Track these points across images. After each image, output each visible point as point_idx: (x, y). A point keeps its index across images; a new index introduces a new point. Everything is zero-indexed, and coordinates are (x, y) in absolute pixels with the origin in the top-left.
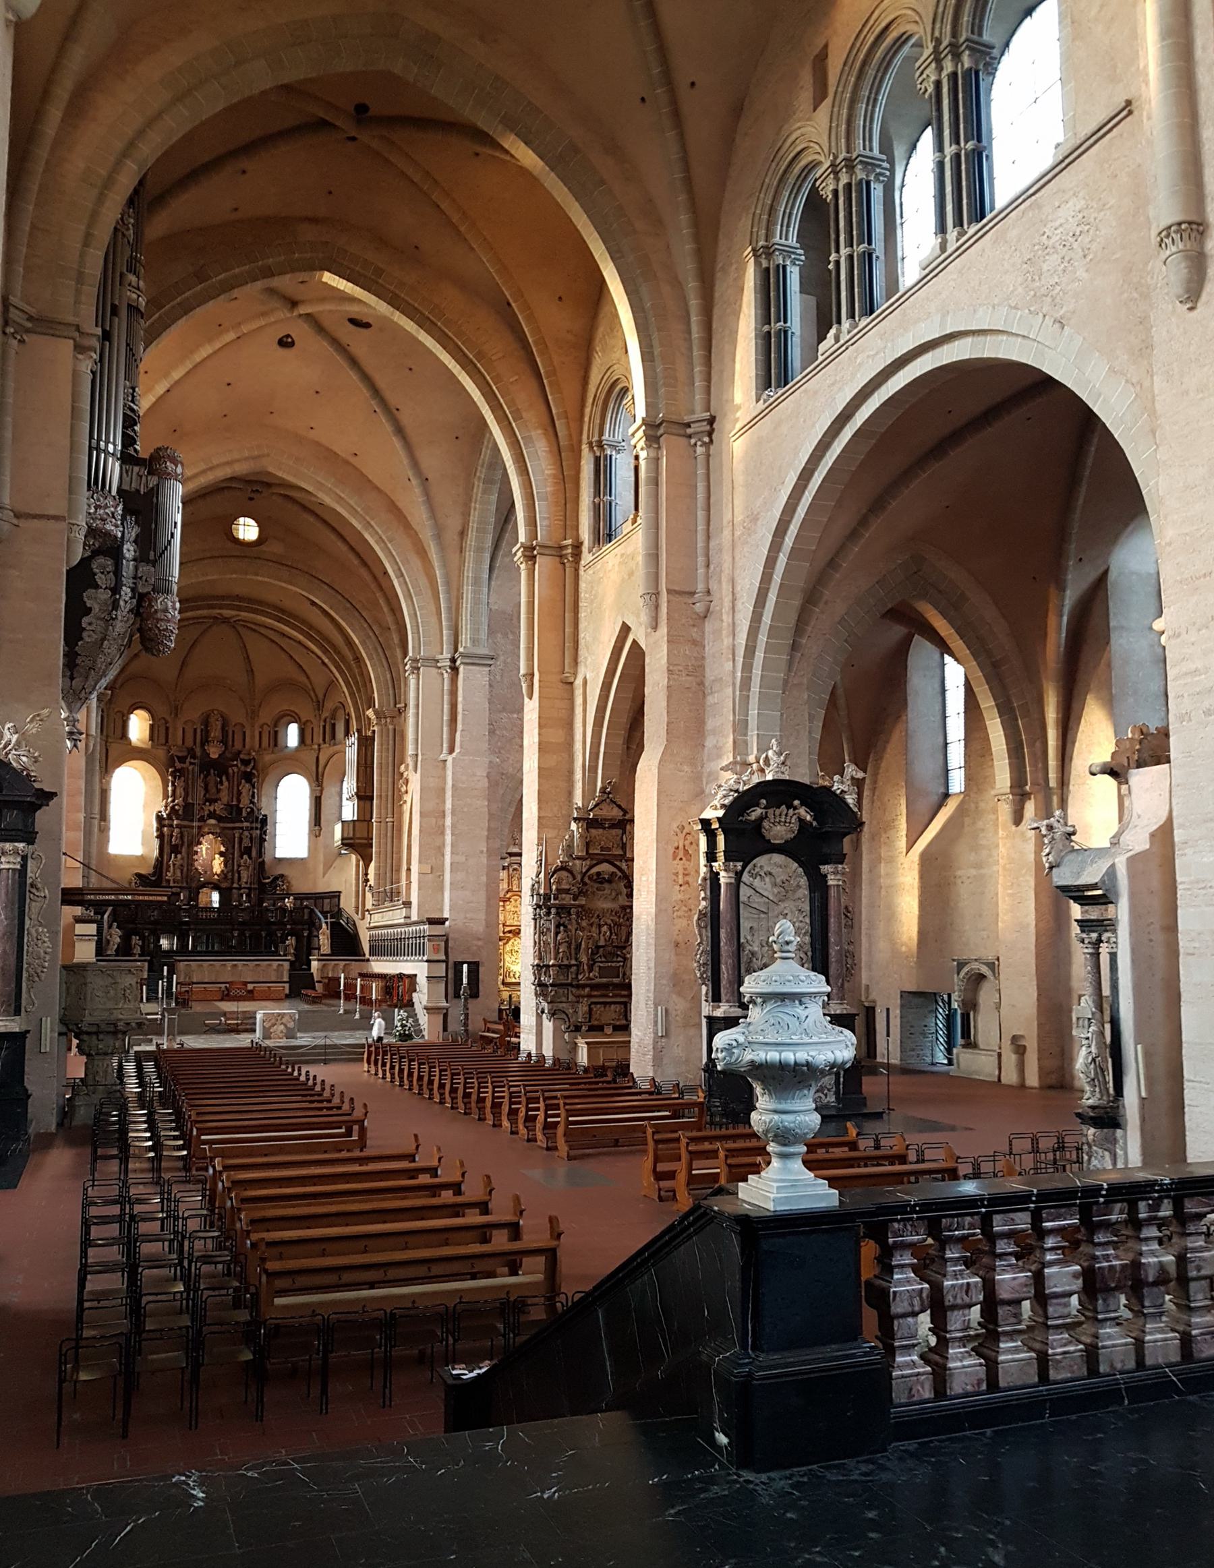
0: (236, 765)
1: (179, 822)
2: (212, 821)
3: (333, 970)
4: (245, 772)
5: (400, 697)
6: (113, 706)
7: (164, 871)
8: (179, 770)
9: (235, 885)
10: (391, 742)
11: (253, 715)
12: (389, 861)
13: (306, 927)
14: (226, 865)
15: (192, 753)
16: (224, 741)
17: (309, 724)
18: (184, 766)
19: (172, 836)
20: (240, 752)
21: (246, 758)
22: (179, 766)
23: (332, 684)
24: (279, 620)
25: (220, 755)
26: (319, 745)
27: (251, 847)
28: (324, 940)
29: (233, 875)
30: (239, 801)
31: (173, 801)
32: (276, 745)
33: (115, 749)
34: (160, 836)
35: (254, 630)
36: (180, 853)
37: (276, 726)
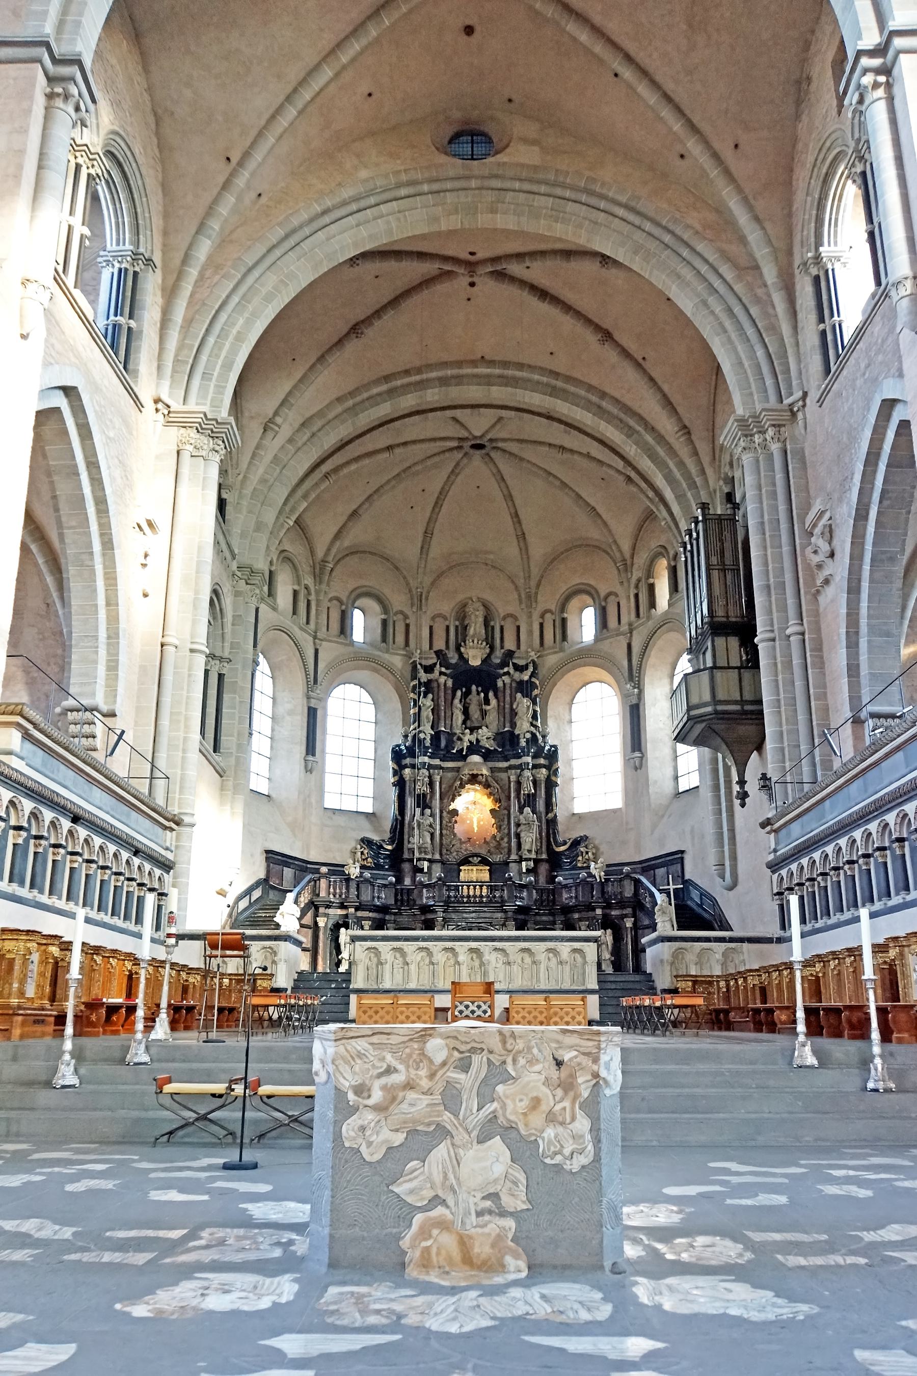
0: (508, 673)
1: (426, 759)
2: (476, 758)
4: (521, 683)
5: (790, 386)
7: (406, 837)
10: (779, 476)
11: (530, 599)
12: (802, 717)
13: (629, 911)
14: (499, 828)
15: (445, 662)
16: (489, 641)
17: (612, 598)
18: (430, 676)
20: (510, 654)
21: (522, 662)
22: (423, 676)
25: (484, 661)
26: (630, 624)
27: (534, 795)
29: (509, 842)
30: (513, 725)
32: (564, 637)
34: (400, 784)
35: (522, 459)
37: (563, 608)
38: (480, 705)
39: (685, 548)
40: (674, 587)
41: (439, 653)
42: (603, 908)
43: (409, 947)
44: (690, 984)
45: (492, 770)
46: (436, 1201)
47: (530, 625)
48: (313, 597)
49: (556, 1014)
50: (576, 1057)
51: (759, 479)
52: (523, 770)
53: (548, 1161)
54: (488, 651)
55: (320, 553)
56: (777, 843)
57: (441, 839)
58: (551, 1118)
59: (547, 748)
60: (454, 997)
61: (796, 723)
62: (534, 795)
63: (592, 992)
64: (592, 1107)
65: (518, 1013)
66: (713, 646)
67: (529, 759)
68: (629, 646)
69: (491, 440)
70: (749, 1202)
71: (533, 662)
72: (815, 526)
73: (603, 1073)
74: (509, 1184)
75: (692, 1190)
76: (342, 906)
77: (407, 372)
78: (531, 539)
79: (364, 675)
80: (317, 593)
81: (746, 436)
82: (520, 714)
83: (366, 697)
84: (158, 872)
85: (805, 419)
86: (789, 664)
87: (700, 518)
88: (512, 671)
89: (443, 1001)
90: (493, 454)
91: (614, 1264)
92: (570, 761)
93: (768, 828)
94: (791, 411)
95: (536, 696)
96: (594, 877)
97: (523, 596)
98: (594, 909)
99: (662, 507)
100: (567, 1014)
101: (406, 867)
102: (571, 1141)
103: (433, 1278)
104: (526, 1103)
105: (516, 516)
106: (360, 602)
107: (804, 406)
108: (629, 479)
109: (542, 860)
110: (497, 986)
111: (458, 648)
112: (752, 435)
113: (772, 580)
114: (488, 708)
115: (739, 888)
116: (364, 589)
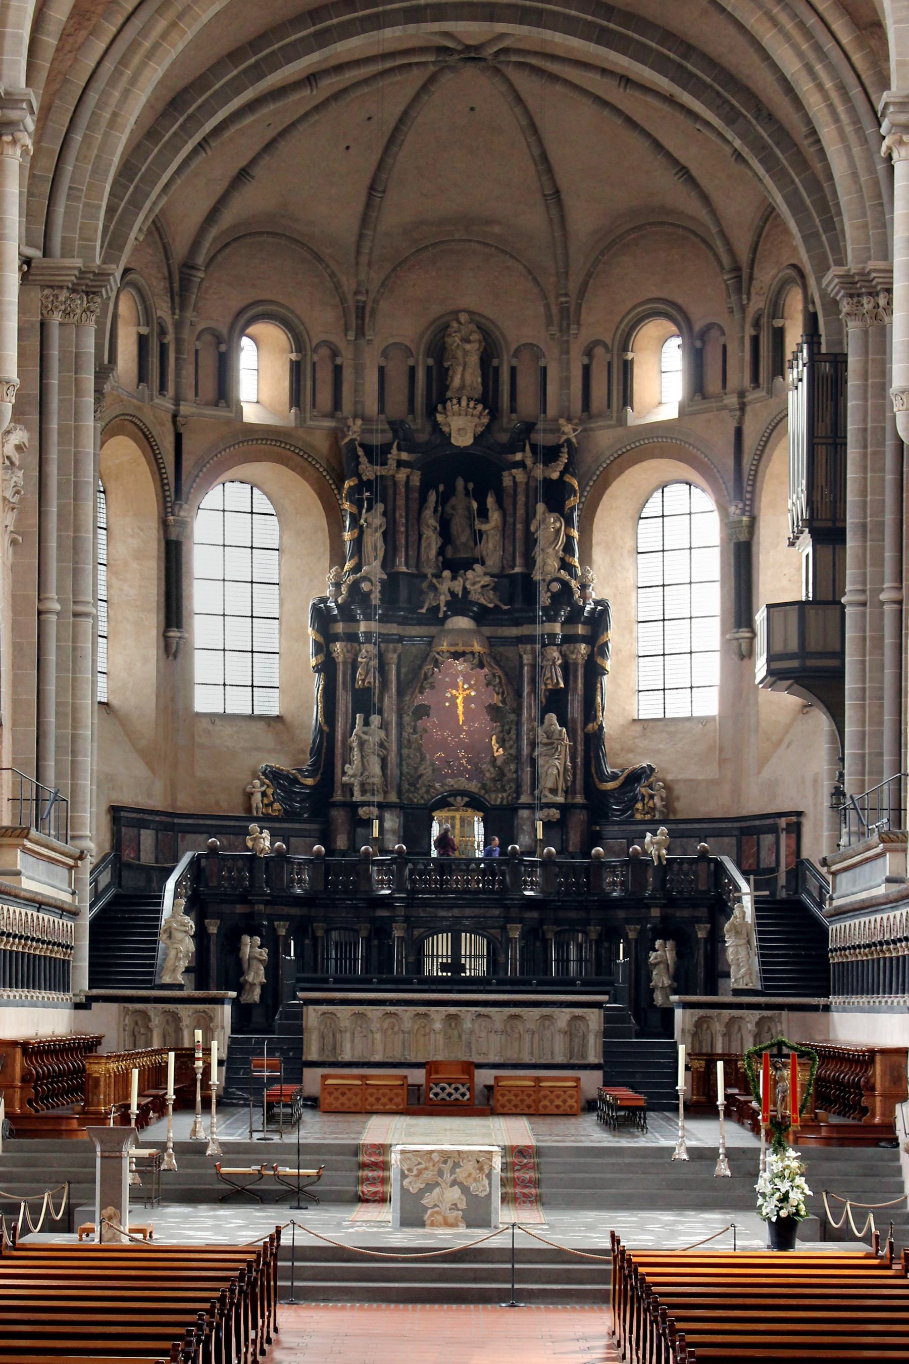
0: (521, 464)
1: (374, 626)
2: (462, 622)
3: (727, 1035)
4: (547, 482)
6: (189, 314)
8: (367, 485)
9: (524, 799)
13: (703, 912)
17: (714, 333)
18: (379, 470)
19: (355, 666)
22: (368, 471)
23: (769, 213)
24: (603, 37)
25: (477, 438)
26: (742, 394)
27: (566, 690)
30: (530, 562)
31: (357, 569)
32: (627, 399)
34: (327, 668)
35: (554, 78)
36: (380, 712)
37: (625, 348)
38: (470, 518)
42: (663, 907)
43: (374, 1012)
44: (703, 1063)
45: (491, 642)
46: (436, 1206)
47: (566, 366)
48: (170, 338)
49: (545, 1097)
51: (866, 362)
54: (486, 420)
55: (180, 246)
57: (400, 765)
59: (588, 608)
60: (429, 1074)
61: (881, 723)
62: (566, 690)
65: (503, 1095)
67: (557, 628)
68: (739, 433)
71: (568, 441)
76: (243, 899)
78: (569, 201)
80: (178, 326)
82: (542, 543)
83: (262, 503)
86: (879, 641)
89: (418, 1076)
90: (502, 67)
97: (555, 310)
98: (648, 907)
100: (558, 1097)
101: (339, 816)
105: (544, 161)
106: (251, 330)
109: (575, 806)
111: (431, 412)
114: (485, 527)
116: (260, 309)
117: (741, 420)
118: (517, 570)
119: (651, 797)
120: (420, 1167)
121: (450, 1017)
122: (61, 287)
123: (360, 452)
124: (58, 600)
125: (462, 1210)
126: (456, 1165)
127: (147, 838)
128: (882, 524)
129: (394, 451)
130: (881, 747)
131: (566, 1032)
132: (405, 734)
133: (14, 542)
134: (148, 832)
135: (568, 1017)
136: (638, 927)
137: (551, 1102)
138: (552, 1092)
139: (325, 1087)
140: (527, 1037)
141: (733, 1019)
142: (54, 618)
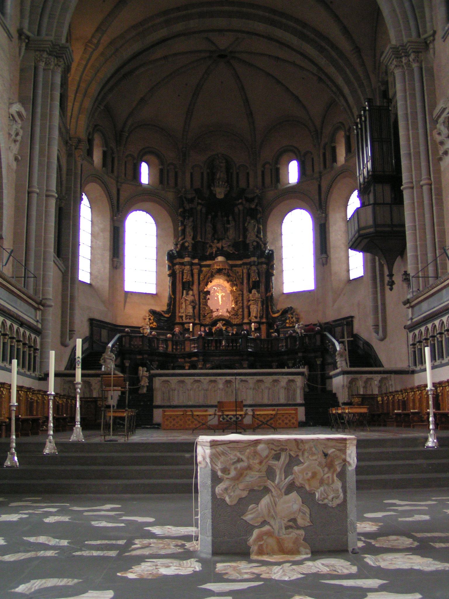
0: (241, 203)
2: (220, 259)
3: (365, 387)
5: (425, 27)
9: (246, 321)
12: (429, 236)
20: (243, 191)
21: (250, 196)
22: (188, 206)
25: (226, 195)
26: (320, 173)
28: (342, 364)
29: (243, 311)
30: (245, 237)
31: (184, 239)
32: (278, 180)
33: (127, 190)
34: (173, 275)
36: (192, 290)
39: (357, 126)
40: (349, 150)
41: (198, 191)
44: (360, 399)
46: (264, 523)
50: (334, 452)
52: (251, 266)
53: (320, 502)
54: (228, 189)
56: (412, 314)
58: (322, 482)
59: (267, 252)
63: (300, 405)
64: (342, 475)
66: (374, 190)
68: (320, 186)
69: (231, 52)
70: (410, 519)
72: (439, 117)
73: (348, 459)
74: (301, 514)
75: (379, 515)
77: (178, 9)
79: (149, 205)
81: (397, 58)
84: (33, 336)
85: (434, 48)
86: (421, 204)
87: (367, 108)
88: (244, 202)
91: (353, 549)
92: (281, 259)
93: (408, 305)
94: (426, 42)
95: (260, 218)
96: (297, 333)
98: (297, 353)
99: (341, 98)
100: (286, 418)
102: (332, 493)
103: (265, 558)
104: (310, 474)
105: (246, 101)
106: (145, 158)
107: (434, 40)
108: (320, 79)
109: (263, 323)
110: (245, 403)
111: (209, 187)
112: (401, 58)
113: (412, 151)
114: (228, 226)
115: (387, 339)
117: (320, 182)
118: (240, 240)
119: (292, 318)
120: (239, 465)
121: (227, 382)
122: (44, 51)
123: (184, 200)
124: (38, 188)
125: (304, 528)
126: (293, 461)
127: (104, 333)
128: (419, 152)
129: (196, 199)
130: (426, 251)
131: (286, 388)
132: (201, 299)
133: (16, 159)
134: (105, 330)
135: (286, 380)
136: (293, 362)
137: (283, 421)
138: (283, 416)
139: (164, 416)
140: (266, 391)
141: (368, 380)
142: (35, 195)
